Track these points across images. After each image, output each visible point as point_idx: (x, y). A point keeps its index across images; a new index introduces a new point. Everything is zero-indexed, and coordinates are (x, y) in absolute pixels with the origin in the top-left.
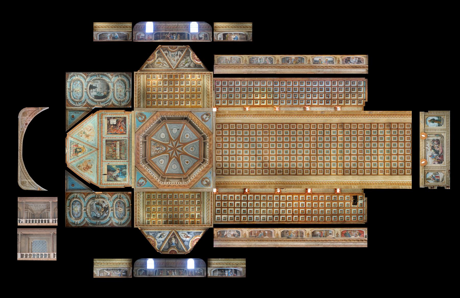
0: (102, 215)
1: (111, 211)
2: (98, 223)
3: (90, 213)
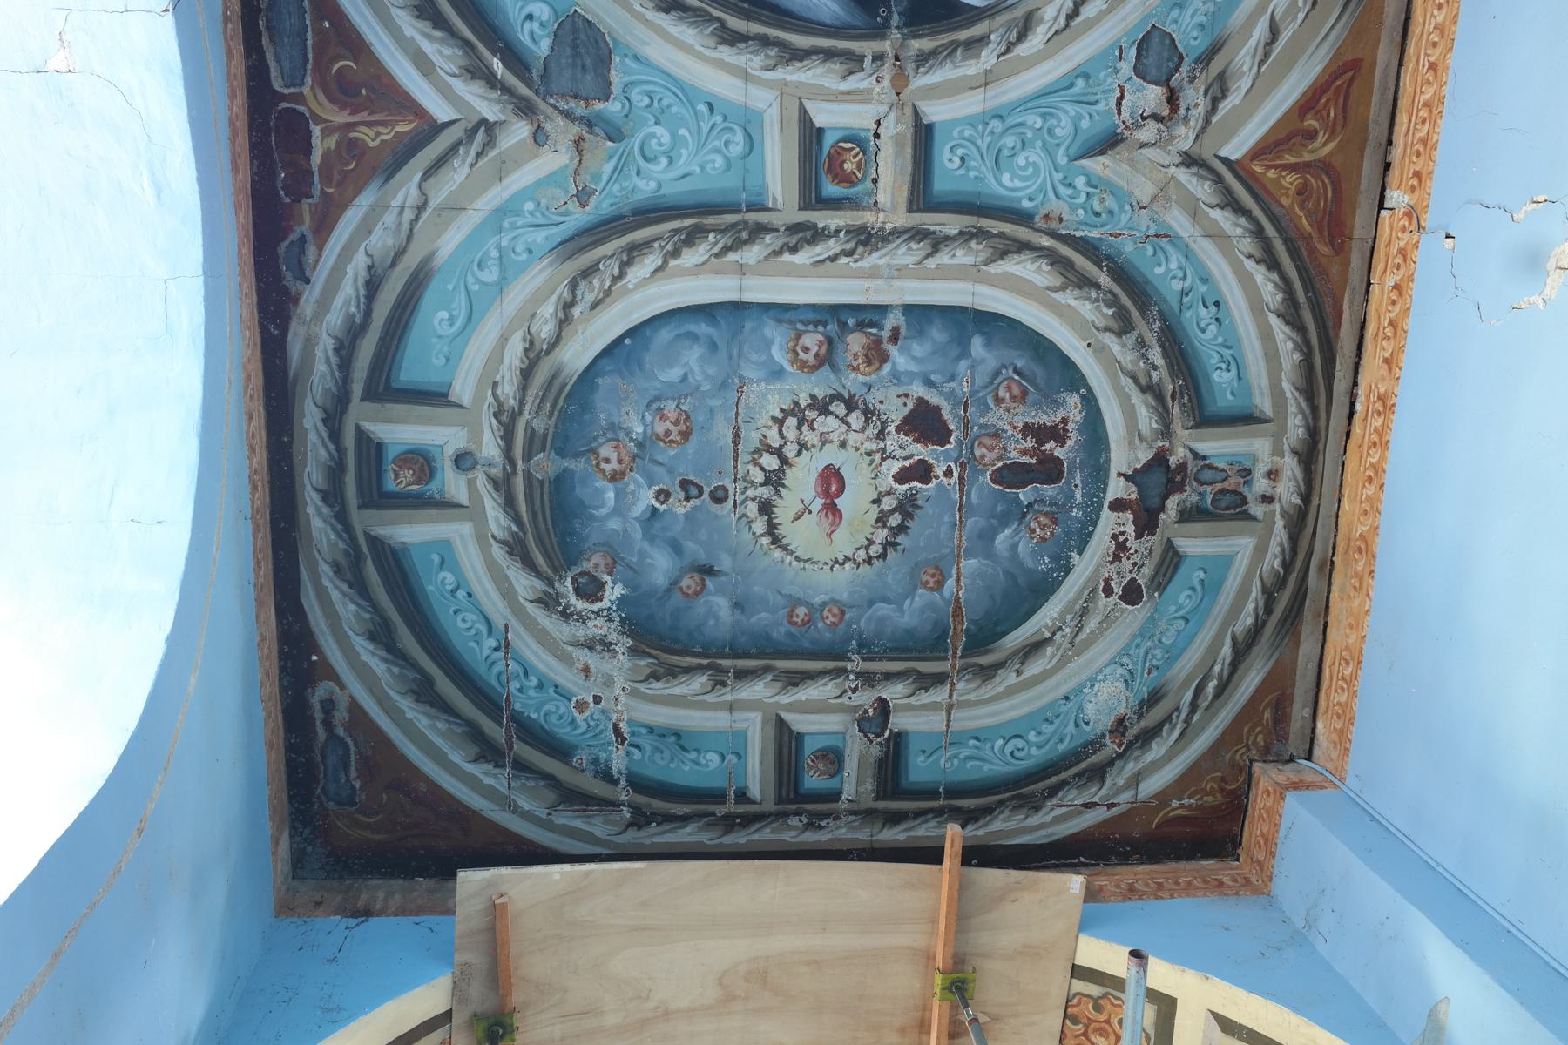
1: (811, 135)
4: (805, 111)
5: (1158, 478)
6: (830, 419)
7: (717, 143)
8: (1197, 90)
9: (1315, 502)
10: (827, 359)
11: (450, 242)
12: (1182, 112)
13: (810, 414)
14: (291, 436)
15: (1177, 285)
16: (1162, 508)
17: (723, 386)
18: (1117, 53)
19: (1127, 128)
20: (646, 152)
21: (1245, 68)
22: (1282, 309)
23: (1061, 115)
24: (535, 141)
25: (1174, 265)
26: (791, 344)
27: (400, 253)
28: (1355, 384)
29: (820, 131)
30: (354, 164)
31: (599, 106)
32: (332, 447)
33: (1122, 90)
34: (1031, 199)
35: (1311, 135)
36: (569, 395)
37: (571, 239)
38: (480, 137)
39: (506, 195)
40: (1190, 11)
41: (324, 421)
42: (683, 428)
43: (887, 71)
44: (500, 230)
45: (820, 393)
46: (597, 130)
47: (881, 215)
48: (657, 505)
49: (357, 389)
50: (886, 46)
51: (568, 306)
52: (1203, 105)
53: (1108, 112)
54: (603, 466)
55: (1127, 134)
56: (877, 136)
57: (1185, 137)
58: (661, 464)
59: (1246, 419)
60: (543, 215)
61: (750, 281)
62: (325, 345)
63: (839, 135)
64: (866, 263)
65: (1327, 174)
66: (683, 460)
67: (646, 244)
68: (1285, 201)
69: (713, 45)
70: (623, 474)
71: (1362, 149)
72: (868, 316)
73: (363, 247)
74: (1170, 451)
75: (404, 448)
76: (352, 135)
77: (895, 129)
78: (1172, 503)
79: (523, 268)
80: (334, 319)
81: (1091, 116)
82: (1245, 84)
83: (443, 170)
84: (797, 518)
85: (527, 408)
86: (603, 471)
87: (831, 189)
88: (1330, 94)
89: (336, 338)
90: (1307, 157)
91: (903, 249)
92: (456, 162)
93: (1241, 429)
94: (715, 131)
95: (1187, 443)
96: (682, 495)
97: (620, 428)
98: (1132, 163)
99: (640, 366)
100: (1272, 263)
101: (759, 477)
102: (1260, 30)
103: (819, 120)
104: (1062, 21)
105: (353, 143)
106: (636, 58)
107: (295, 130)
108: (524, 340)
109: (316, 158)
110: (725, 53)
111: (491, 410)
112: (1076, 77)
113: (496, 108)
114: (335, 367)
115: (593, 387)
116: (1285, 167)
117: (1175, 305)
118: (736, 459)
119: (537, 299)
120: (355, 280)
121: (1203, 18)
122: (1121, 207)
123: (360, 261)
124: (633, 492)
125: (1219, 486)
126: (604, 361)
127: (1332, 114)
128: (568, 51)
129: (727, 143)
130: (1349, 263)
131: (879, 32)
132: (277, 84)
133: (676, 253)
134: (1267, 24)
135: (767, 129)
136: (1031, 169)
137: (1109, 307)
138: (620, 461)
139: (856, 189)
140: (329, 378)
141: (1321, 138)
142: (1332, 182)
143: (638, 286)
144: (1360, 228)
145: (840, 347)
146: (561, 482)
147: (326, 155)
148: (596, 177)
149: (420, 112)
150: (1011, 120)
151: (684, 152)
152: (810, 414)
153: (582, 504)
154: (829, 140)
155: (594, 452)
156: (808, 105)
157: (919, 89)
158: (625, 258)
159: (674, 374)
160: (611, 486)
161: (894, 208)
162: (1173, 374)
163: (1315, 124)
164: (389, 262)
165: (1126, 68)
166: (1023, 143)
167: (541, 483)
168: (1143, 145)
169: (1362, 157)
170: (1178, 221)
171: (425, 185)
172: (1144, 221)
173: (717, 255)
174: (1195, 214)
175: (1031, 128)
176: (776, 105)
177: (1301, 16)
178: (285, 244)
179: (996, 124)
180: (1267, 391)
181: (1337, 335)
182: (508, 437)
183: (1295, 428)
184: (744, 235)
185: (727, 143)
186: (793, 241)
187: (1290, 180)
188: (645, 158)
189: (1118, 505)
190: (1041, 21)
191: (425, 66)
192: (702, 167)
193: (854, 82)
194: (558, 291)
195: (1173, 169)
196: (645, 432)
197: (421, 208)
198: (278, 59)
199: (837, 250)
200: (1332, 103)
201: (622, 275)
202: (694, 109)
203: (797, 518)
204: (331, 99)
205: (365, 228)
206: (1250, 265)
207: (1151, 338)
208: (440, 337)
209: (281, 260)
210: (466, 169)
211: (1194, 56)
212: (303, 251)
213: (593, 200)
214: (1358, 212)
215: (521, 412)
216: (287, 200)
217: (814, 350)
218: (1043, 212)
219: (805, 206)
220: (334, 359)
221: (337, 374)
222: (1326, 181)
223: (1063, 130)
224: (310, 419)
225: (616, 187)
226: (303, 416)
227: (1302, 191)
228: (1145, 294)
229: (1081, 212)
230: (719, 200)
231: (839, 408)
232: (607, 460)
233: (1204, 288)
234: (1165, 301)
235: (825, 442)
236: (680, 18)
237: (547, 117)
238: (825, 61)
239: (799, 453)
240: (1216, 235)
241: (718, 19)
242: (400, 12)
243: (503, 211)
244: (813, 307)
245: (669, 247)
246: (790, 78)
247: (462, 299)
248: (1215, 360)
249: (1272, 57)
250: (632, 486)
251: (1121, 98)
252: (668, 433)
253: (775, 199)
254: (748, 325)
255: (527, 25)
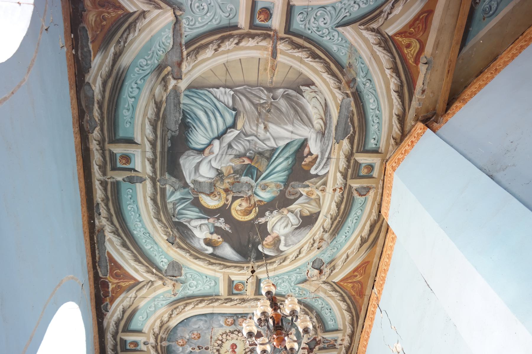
0: (196, 203)
1: (231, 282)
2: (127, 158)
3: (221, 78)
4: (230, 277)
5: (314, 342)
6: (234, 335)
7: (208, 284)
8: (328, 269)
9: (353, 344)
10: (234, 323)
11: (142, 304)
12: (324, 273)
13: (229, 334)
14: (104, 339)
15: (320, 306)
16: (314, 348)
17: (208, 328)
18: (307, 263)
19: (309, 278)
20: (190, 286)
21: (340, 264)
22: (346, 309)
23: (293, 276)
24: (164, 285)
25: (320, 302)
26: (225, 321)
27: (130, 306)
28: (364, 322)
29: (233, 281)
30: (119, 289)
31: (179, 277)
32: (114, 341)
33: (308, 271)
34: (285, 292)
35: (356, 276)
36: (171, 331)
37: (172, 302)
38: (150, 284)
39: (156, 294)
40: (327, 254)
41: (112, 337)
42: (199, 336)
43: (250, 269)
44: (155, 301)
45: (232, 330)
46: (178, 282)
47: (248, 297)
48: (192, 350)
49: (120, 330)
50: (250, 265)
51: (171, 315)
52: (329, 271)
53: (305, 275)
54: (179, 343)
55: (309, 279)
56: (247, 283)
57: (324, 278)
58: (192, 343)
59: (337, 330)
60: (165, 298)
61: (215, 309)
62: (112, 323)
63: (238, 282)
64: (244, 305)
65: (360, 283)
66: (199, 342)
67: (190, 303)
68: (348, 289)
69: (207, 265)
70: (184, 345)
71: (368, 278)
72: (244, 315)
73: (121, 305)
74: (317, 338)
75: (130, 341)
76: (119, 284)
77: (252, 280)
78: (317, 347)
79: (160, 308)
80: (115, 318)
81: (300, 276)
82: (340, 267)
83: (141, 290)
84: (226, 352)
85: (161, 333)
86: (179, 345)
87: (235, 292)
88: (361, 268)
89: (115, 322)
90: (355, 280)
91: (253, 302)
92: (144, 289)
93: (335, 332)
94: (207, 281)
95: (321, 336)
96: (198, 349)
97: (183, 337)
98: (310, 285)
99: (188, 325)
100: (344, 300)
101: (217, 345)
102: (345, 256)
103: (233, 279)
104: (294, 258)
105: (119, 286)
106: (188, 268)
107: (105, 285)
108: (160, 321)
109: (110, 289)
110: (210, 267)
111: (152, 334)
112: (297, 269)
113: (154, 278)
114: (115, 327)
115: (177, 329)
116: (348, 283)
117: (320, 310)
118: (211, 342)
119: (164, 313)
120: (120, 311)
121: (330, 255)
122: (307, 293)
123: (121, 308)
124: (186, 348)
125: (329, 343)
126: (180, 325)
127: (361, 272)
128: (172, 267)
129: (210, 284)
130: (364, 300)
131: (249, 262)
132: (101, 275)
133: (197, 304)
134: (346, 255)
135: (220, 281)
136: (285, 287)
137: (303, 312)
138: (183, 343)
139: (241, 292)
140: (113, 329)
141: (358, 276)
142: (361, 285)
143: (188, 311)
144: (367, 292)
145: (237, 321)
146: (168, 347)
147: (112, 289)
148: (178, 291)
149: (135, 279)
150: (280, 277)
151: (200, 286)
152: (229, 334)
153: (174, 351)
154: (235, 283)
155: (177, 341)
156: (230, 276)
157: (258, 272)
158: (185, 305)
159: (197, 326)
160: (181, 347)
161: (251, 295)
162: (318, 323)
163: (357, 274)
164: (128, 307)
165: (310, 266)
166: (283, 282)
167: (164, 347)
168: (313, 281)
169: (368, 280)
170: (321, 294)
171: (137, 293)
172: (313, 295)
173: (207, 305)
174: (325, 292)
175: (285, 278)
176: (222, 277)
177: (355, 253)
178: (102, 306)
179: (277, 278)
180: (342, 324)
181: (360, 313)
182: (156, 338)
183: (349, 331)
184: (214, 301)
185: (210, 284)
186: (226, 301)
187: (350, 285)
188: (190, 287)
189: (303, 348)
190: (289, 258)
191: (136, 271)
192: (204, 288)
193: (241, 272)
194: (169, 312)
195: (320, 284)
196: (189, 337)
197: (135, 298)
198: (101, 271)
199: (237, 303)
200: (362, 270)
201: (184, 308)
202: (202, 277)
203: (226, 352)
204: (114, 278)
205: (122, 301)
206: (339, 302)
207: (313, 317)
208: (140, 321)
209: (102, 308)
210: (146, 290)
211: (327, 263)
212: (107, 306)
213: (177, 295)
214: (367, 290)
215: (159, 334)
216: (103, 297)
217: (231, 322)
218: (287, 295)
219: (229, 295)
220: (115, 326)
221: (115, 328)
222: (359, 284)
223: (293, 278)
224: (109, 337)
225: (183, 292)
226: (107, 336)
227: (353, 287)
228: (312, 308)
229: (297, 294)
230: (208, 294)
231: (237, 333)
232: (180, 343)
233: (327, 306)
234: (317, 309)
235: (232, 339)
236: (199, 260)
237: (166, 280)
238: (235, 268)
239: (226, 341)
240: (331, 297)
241: (208, 260)
242: (130, 261)
243: (155, 298)
244: (231, 314)
245: (196, 303)
246: (226, 271)
247: (145, 314)
248: (329, 319)
249: (347, 261)
250: (186, 347)
251: (308, 272)
252: (195, 337)
253: (222, 294)
254: (215, 317)
255: (162, 263)
